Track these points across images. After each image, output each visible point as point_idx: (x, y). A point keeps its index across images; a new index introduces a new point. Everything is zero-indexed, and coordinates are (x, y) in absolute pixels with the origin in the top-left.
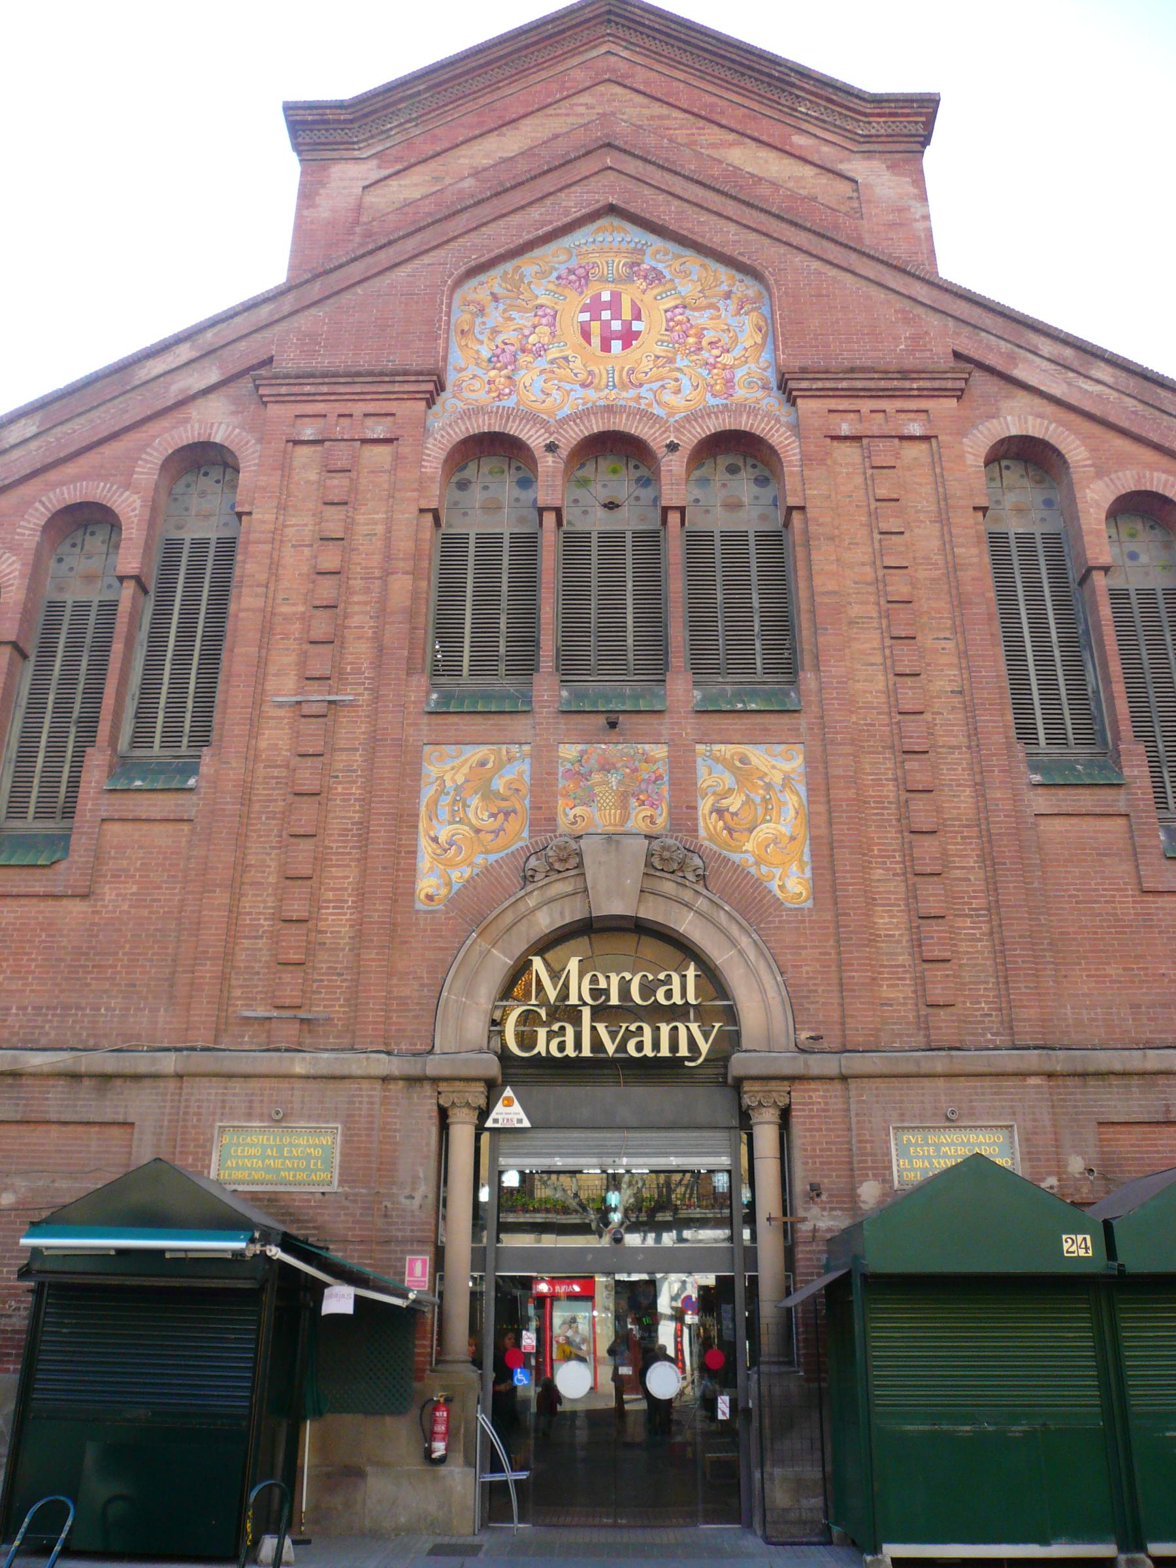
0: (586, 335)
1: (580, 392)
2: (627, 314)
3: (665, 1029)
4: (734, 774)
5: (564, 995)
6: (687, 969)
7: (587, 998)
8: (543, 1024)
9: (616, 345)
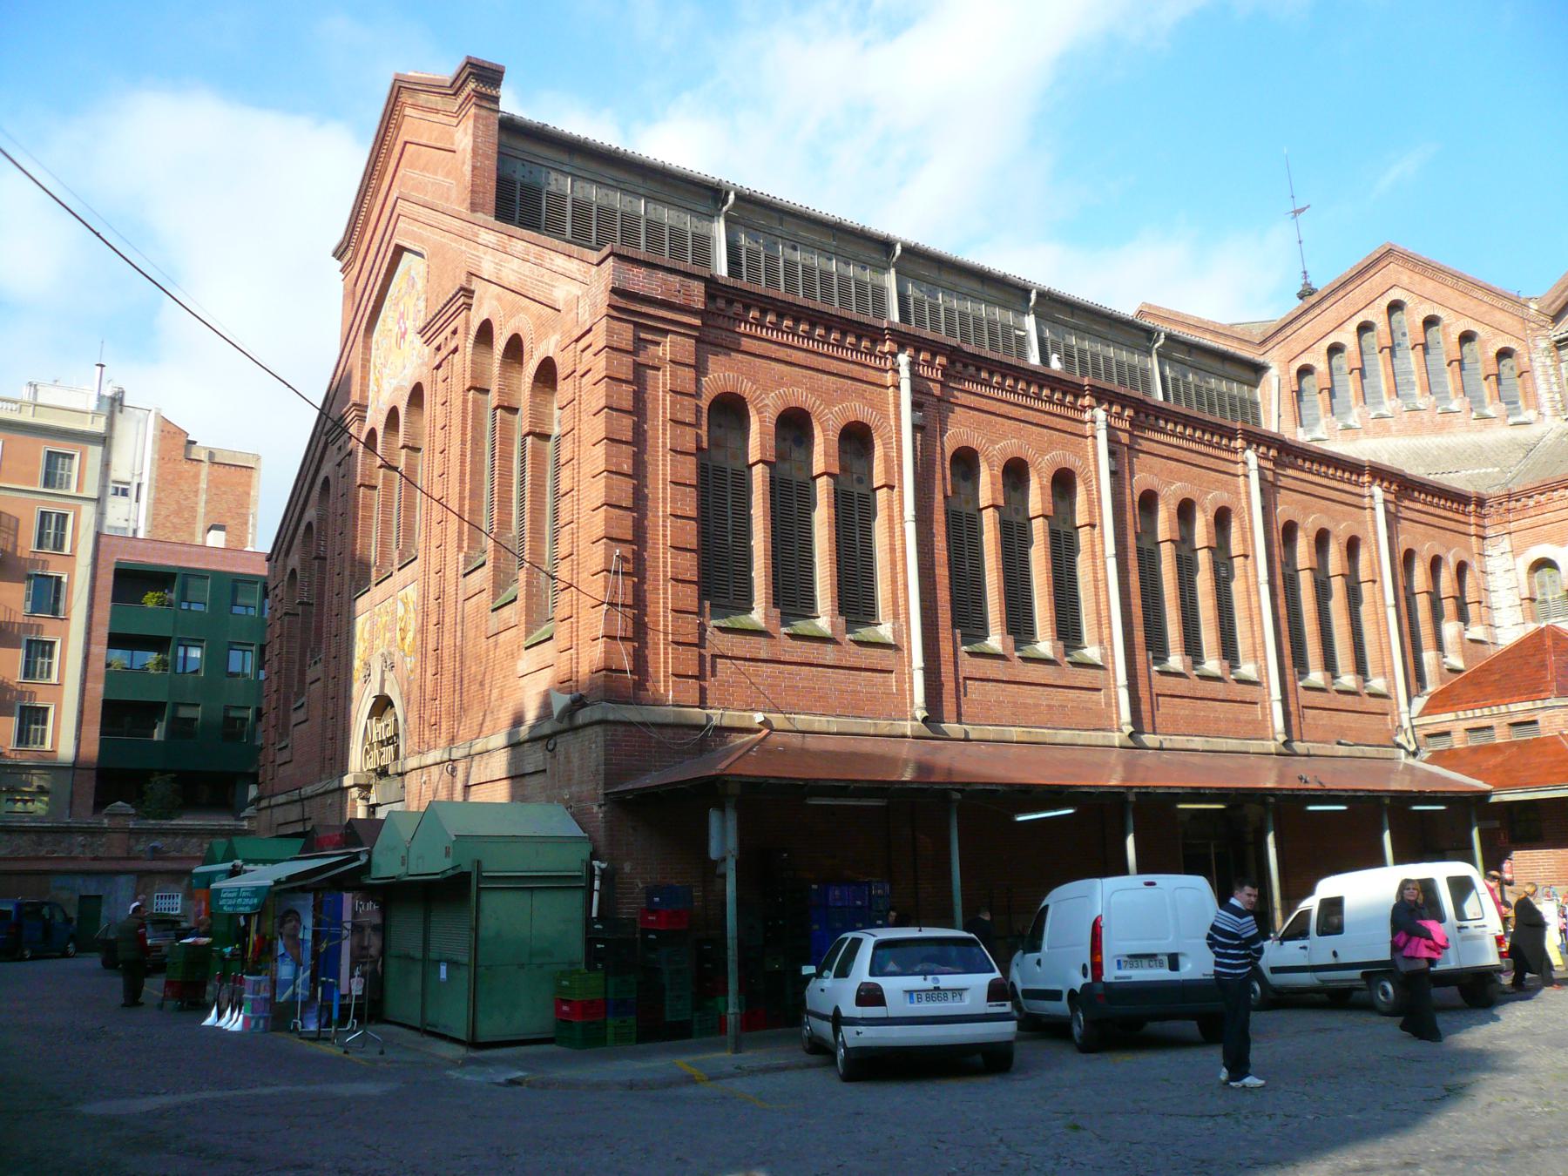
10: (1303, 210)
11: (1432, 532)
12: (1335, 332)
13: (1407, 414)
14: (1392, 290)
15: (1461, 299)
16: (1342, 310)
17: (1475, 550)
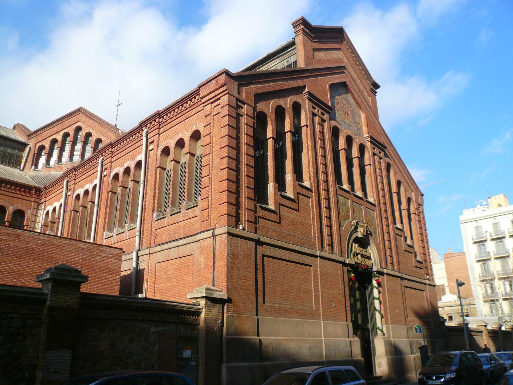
9: (346, 114)
10: (120, 104)
11: (2, 197)
12: (55, 135)
13: (70, 164)
14: (78, 123)
15: (99, 128)
16: (59, 127)
17: (32, 207)
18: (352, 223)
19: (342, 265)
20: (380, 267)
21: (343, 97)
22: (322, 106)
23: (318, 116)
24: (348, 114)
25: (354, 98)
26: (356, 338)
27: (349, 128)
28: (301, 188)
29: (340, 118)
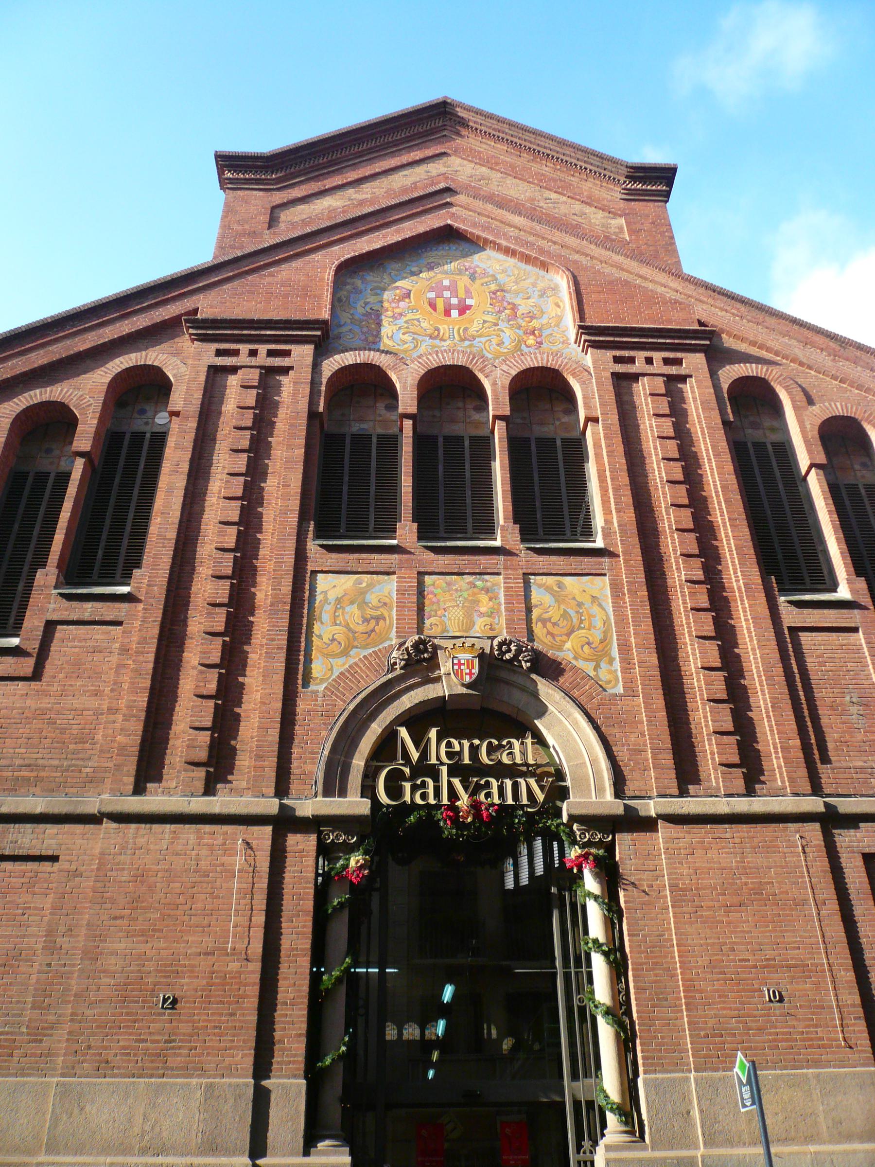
0: (433, 306)
1: (429, 342)
2: (462, 294)
3: (508, 783)
4: (554, 596)
5: (425, 755)
6: (524, 737)
7: (445, 759)
8: (406, 780)
9: (455, 313)
18: (395, 654)
19: (269, 829)
20: (609, 795)
21: (446, 273)
22: (268, 332)
23: (241, 367)
24: (463, 309)
25: (507, 251)
26: (335, 1154)
27: (467, 343)
28: (74, 604)
29: (404, 334)
